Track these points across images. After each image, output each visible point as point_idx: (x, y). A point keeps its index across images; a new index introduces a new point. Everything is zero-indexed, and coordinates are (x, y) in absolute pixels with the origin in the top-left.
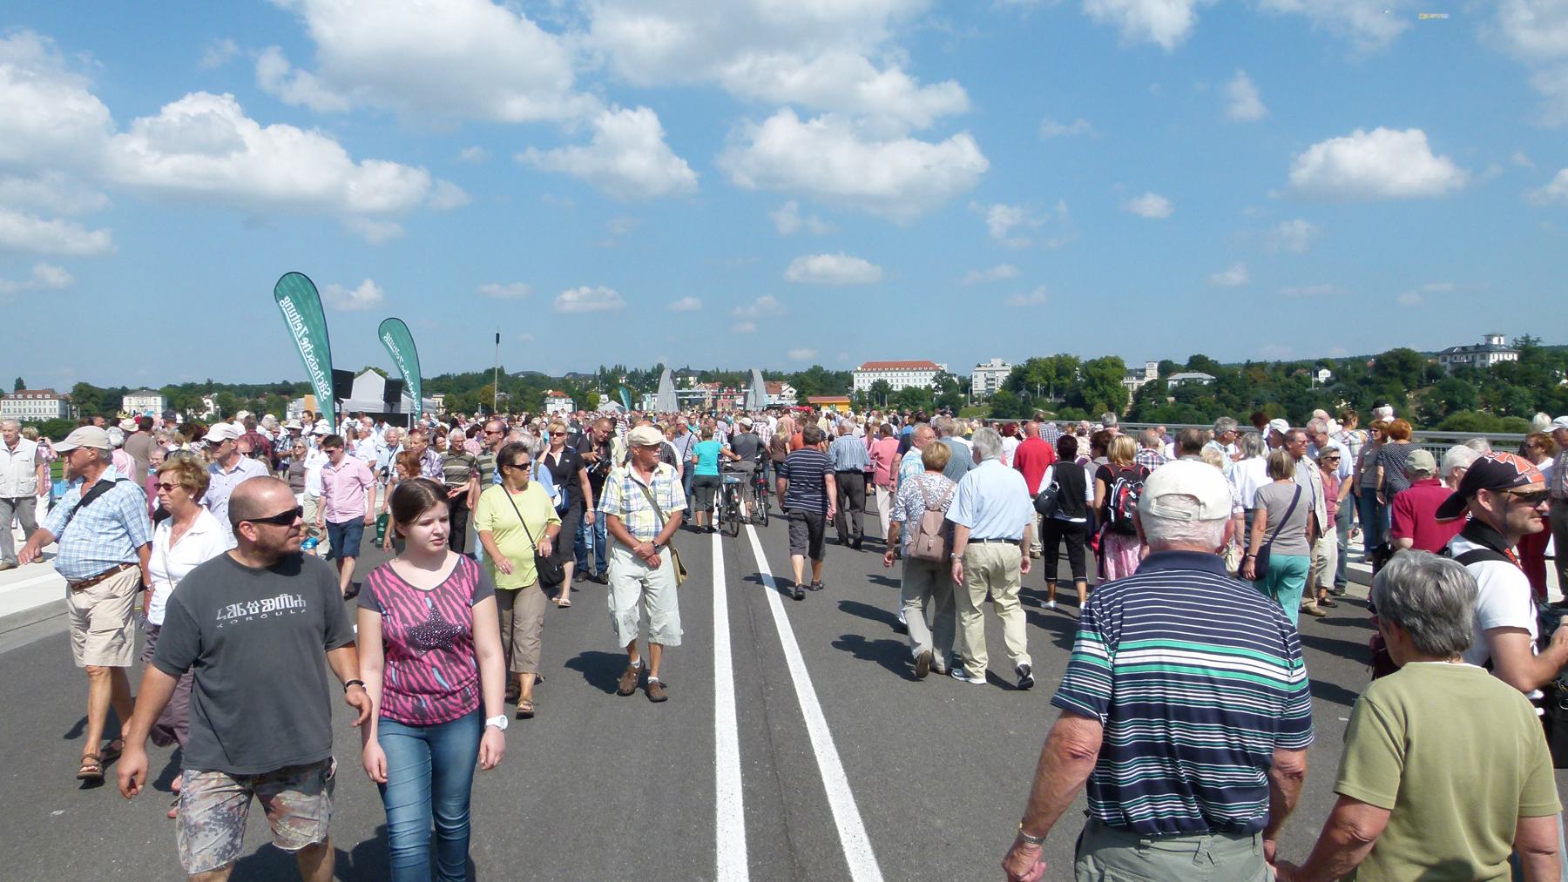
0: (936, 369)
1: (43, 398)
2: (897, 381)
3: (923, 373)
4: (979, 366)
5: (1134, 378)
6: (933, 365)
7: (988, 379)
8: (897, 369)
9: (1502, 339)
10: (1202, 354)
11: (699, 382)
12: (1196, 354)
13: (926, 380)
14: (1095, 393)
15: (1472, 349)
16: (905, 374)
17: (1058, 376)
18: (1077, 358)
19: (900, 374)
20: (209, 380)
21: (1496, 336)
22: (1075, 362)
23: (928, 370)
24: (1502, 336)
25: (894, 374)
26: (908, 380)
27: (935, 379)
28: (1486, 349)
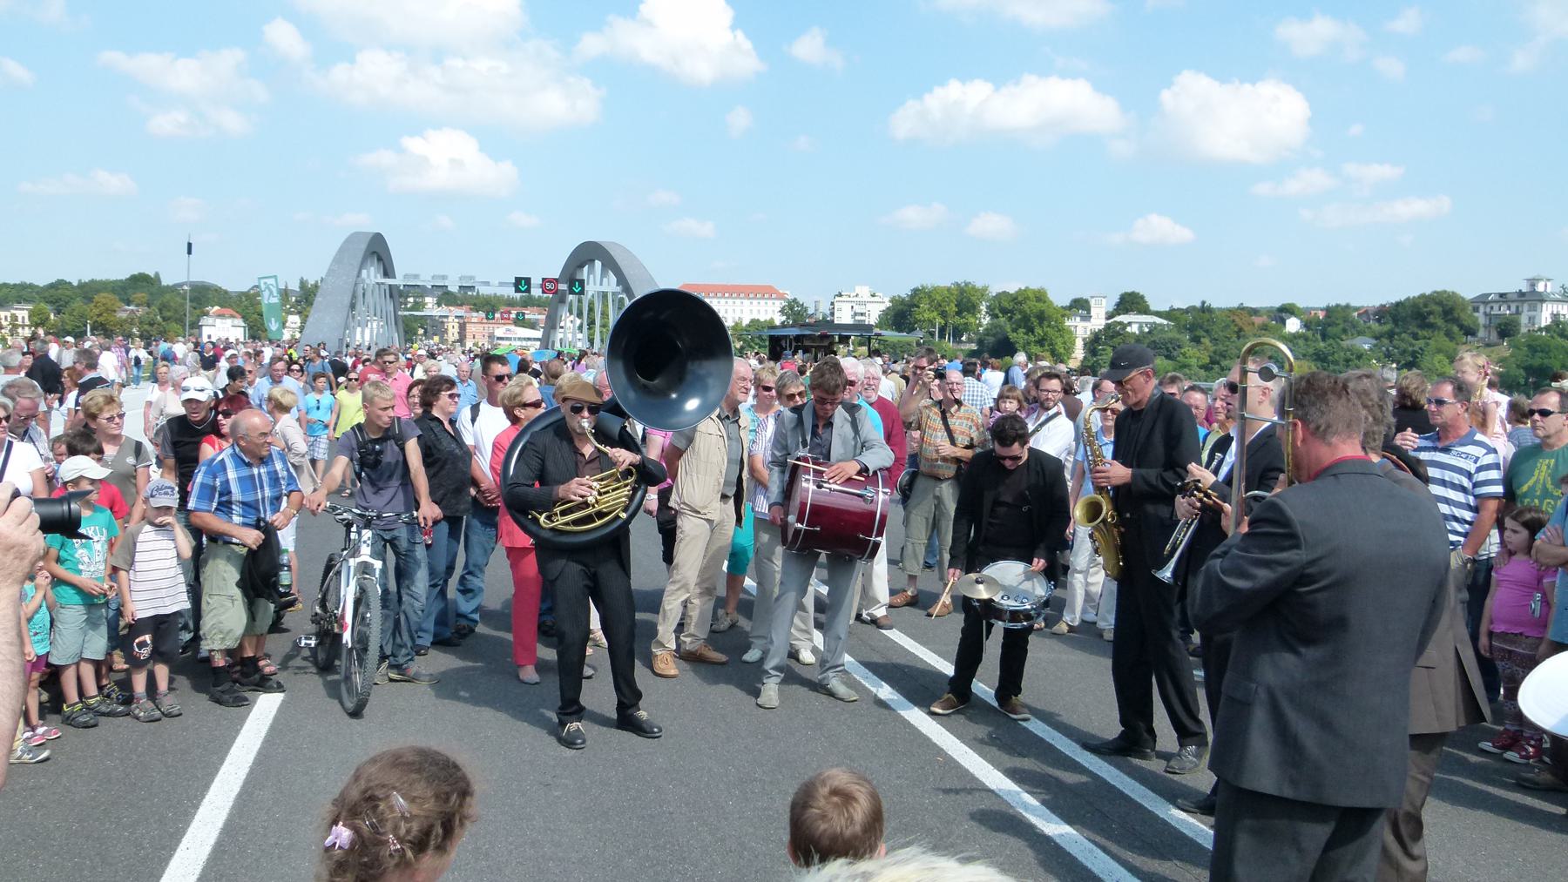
0: (781, 297)
3: (762, 302)
4: (840, 295)
5: (1078, 319)
6: (777, 292)
7: (856, 314)
8: (727, 295)
9: (1549, 284)
10: (1137, 291)
11: (439, 304)
12: (1129, 291)
14: (1032, 338)
15: (1515, 297)
16: (738, 302)
17: (959, 313)
18: (985, 289)
19: (730, 301)
21: (1542, 280)
22: (983, 292)
23: (770, 298)
24: (1549, 280)
26: (742, 311)
27: (782, 311)
28: (1532, 297)
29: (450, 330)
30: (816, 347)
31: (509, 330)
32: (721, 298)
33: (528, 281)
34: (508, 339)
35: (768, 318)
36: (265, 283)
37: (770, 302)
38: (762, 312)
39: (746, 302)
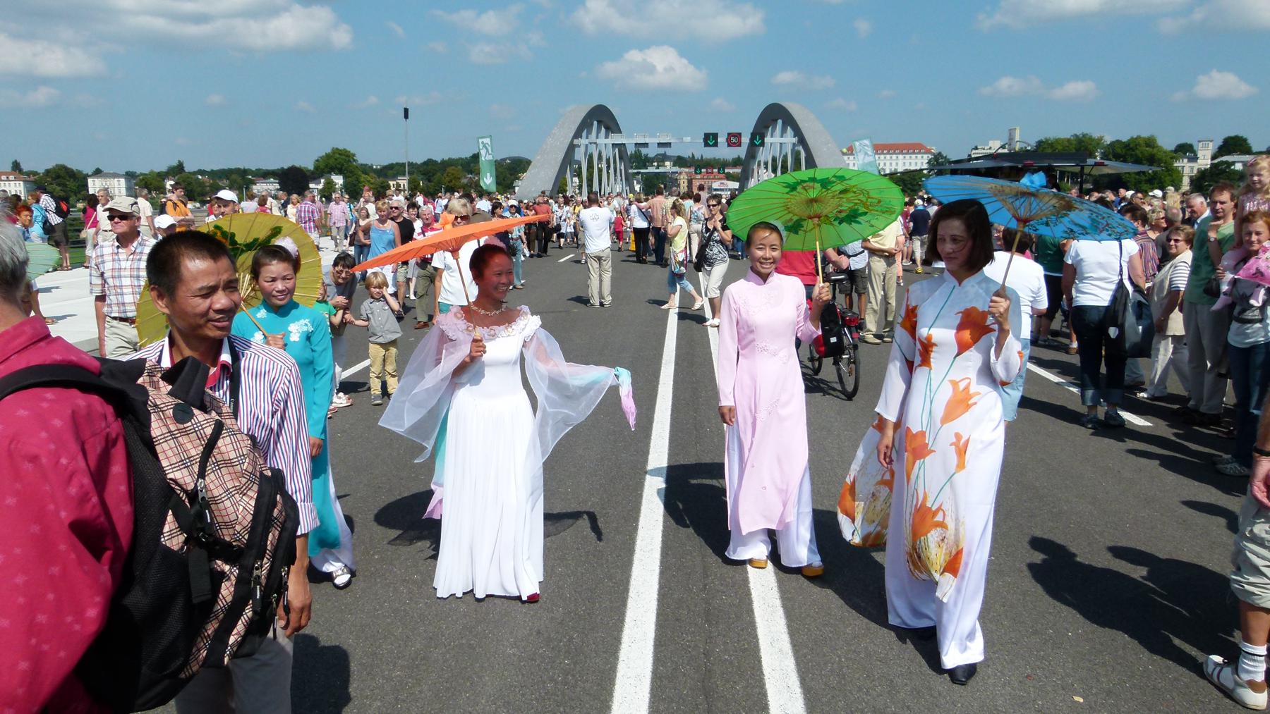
1: (8, 180)
2: (885, 165)
3: (913, 156)
4: (976, 148)
5: (1186, 160)
6: (924, 148)
8: (885, 152)
12: (1232, 134)
13: (916, 163)
16: (894, 157)
18: (1101, 138)
19: (888, 156)
20: (179, 161)
23: (919, 153)
26: (897, 164)
29: (682, 185)
33: (715, 136)
34: (722, 190)
36: (483, 143)
37: (919, 156)
38: (913, 163)
39: (901, 157)
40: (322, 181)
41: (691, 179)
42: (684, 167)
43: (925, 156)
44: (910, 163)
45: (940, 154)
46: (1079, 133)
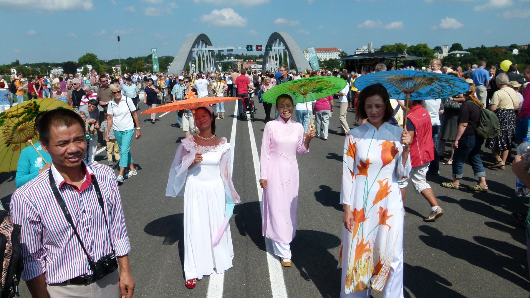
2: (321, 57)
3: (333, 53)
4: (358, 50)
5: (438, 53)
8: (321, 51)
10: (458, 43)
12: (455, 43)
13: (334, 56)
16: (325, 53)
18: (406, 45)
19: (323, 53)
20: (17, 60)
22: (405, 46)
23: (335, 52)
25: (320, 53)
27: (339, 56)
29: (239, 67)
30: (369, 65)
31: (255, 66)
32: (320, 52)
33: (251, 46)
35: (335, 58)
36: (153, 51)
37: (335, 53)
39: (328, 53)
40: (83, 67)
41: (242, 64)
42: (239, 59)
43: (338, 53)
44: (332, 56)
45: (343, 52)
46: (397, 42)
